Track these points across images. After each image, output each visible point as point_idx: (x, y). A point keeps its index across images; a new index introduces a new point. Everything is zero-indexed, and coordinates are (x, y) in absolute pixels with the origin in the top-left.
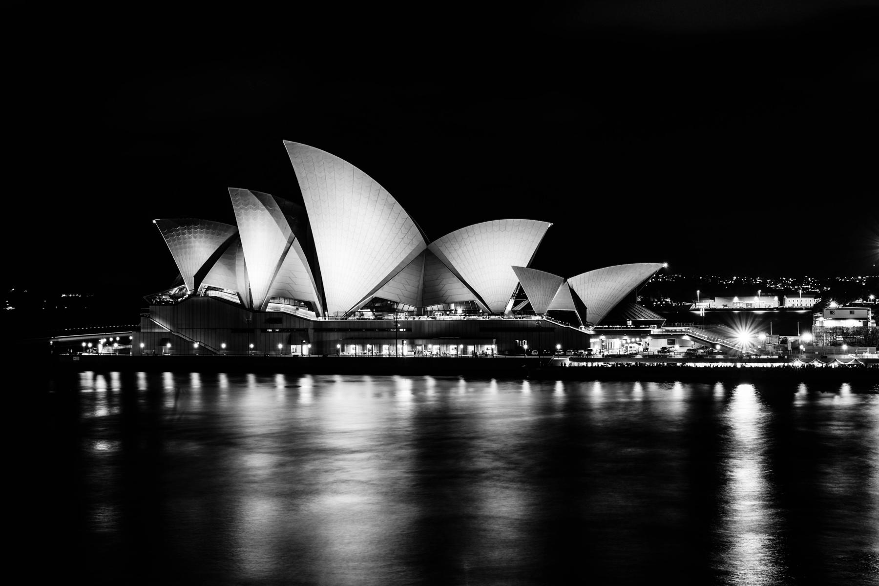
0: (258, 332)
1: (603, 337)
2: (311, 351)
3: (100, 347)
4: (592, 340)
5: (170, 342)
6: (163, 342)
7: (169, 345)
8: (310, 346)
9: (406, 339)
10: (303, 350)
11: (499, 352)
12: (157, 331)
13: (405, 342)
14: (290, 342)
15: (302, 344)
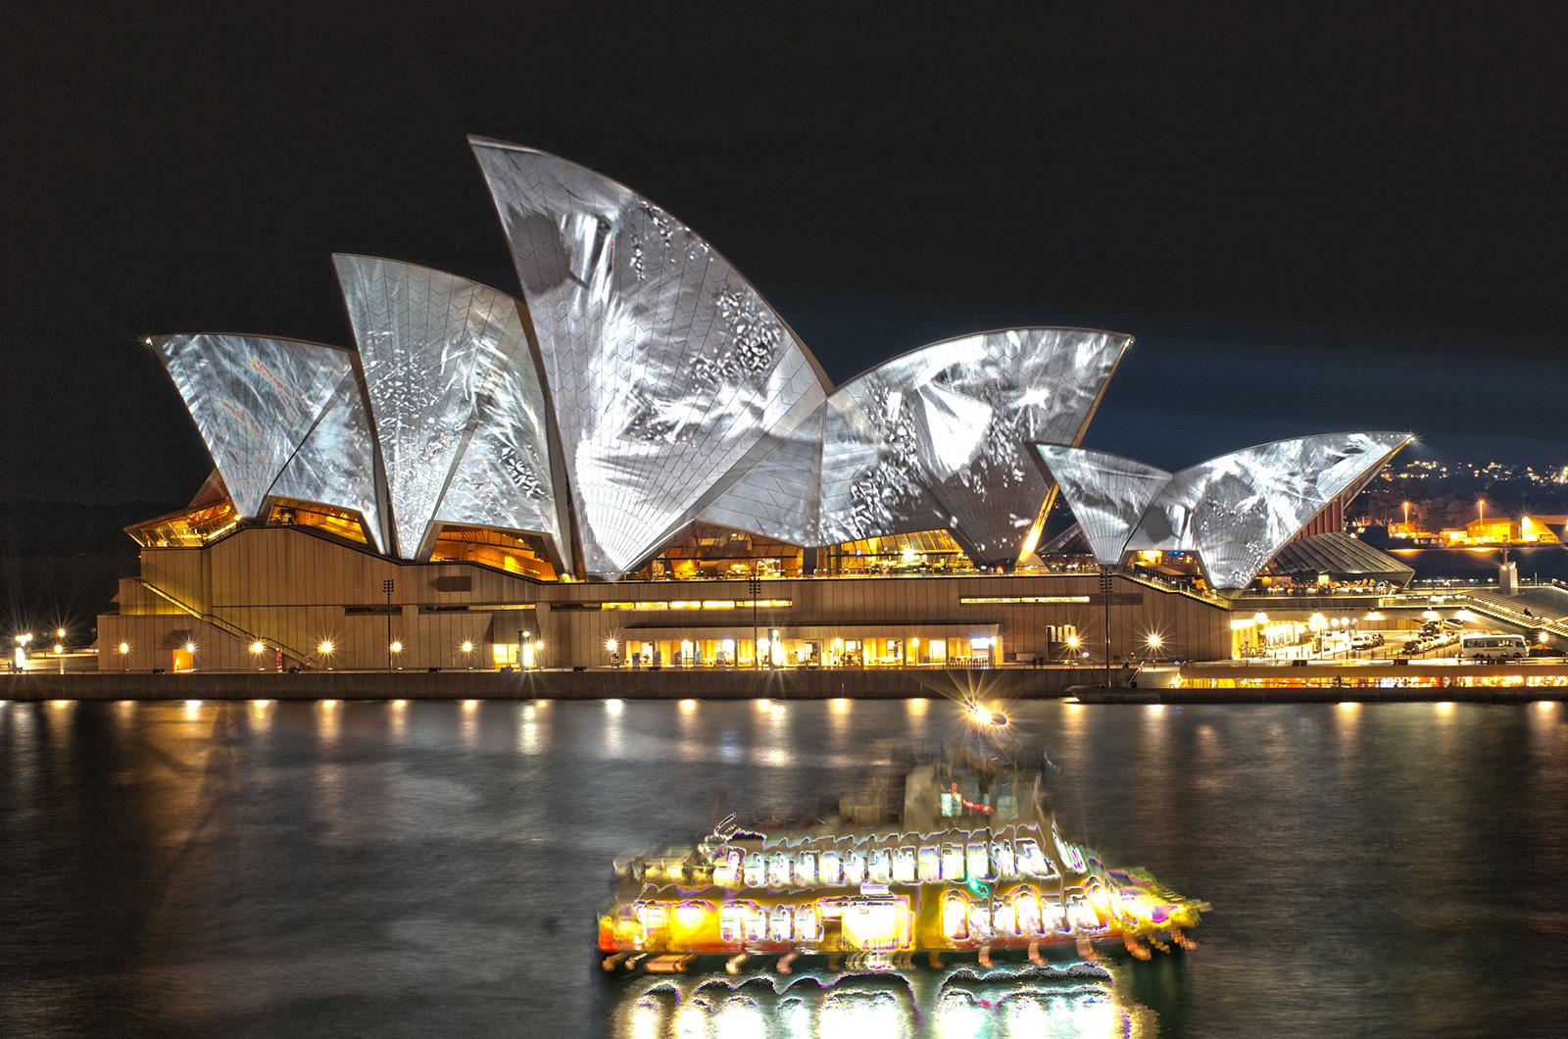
0: (411, 612)
1: (1261, 617)
2: (540, 660)
3: (19, 653)
4: (1238, 625)
5: (194, 640)
6: (176, 639)
7: (191, 648)
8: (540, 645)
9: (778, 624)
10: (522, 655)
11: (1009, 656)
12: (160, 612)
13: (776, 633)
14: (491, 637)
15: (521, 640)
